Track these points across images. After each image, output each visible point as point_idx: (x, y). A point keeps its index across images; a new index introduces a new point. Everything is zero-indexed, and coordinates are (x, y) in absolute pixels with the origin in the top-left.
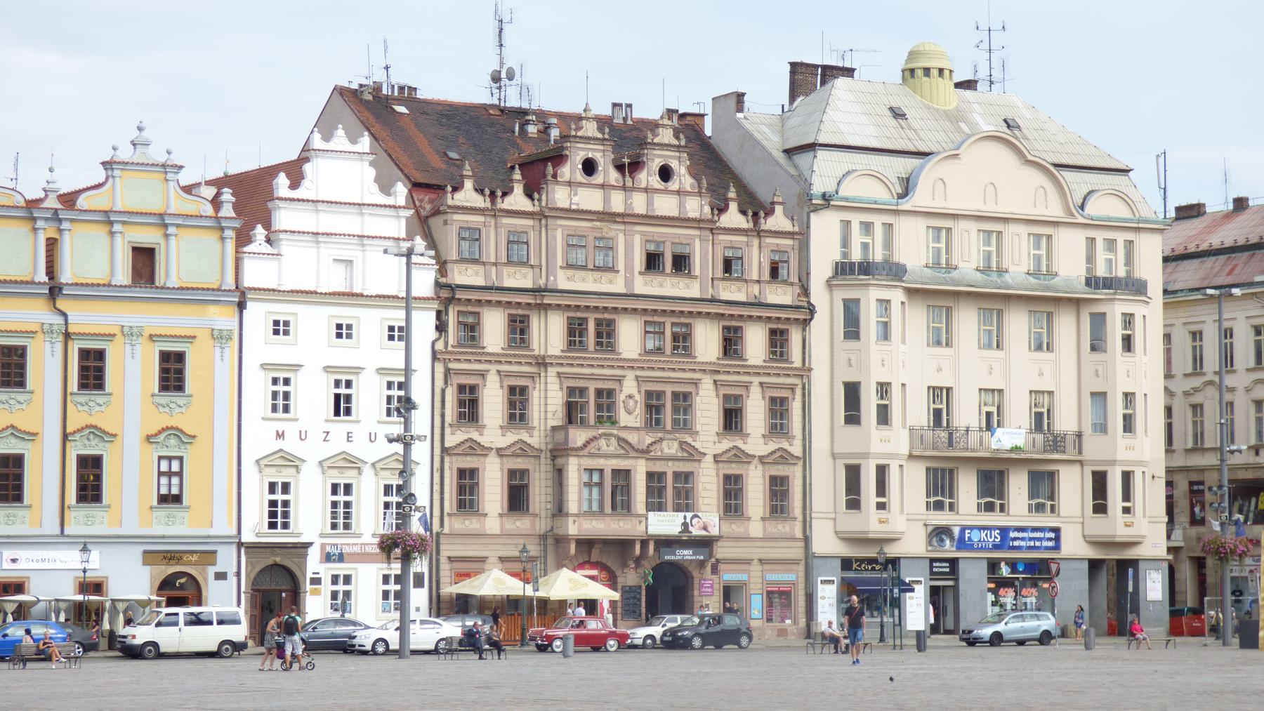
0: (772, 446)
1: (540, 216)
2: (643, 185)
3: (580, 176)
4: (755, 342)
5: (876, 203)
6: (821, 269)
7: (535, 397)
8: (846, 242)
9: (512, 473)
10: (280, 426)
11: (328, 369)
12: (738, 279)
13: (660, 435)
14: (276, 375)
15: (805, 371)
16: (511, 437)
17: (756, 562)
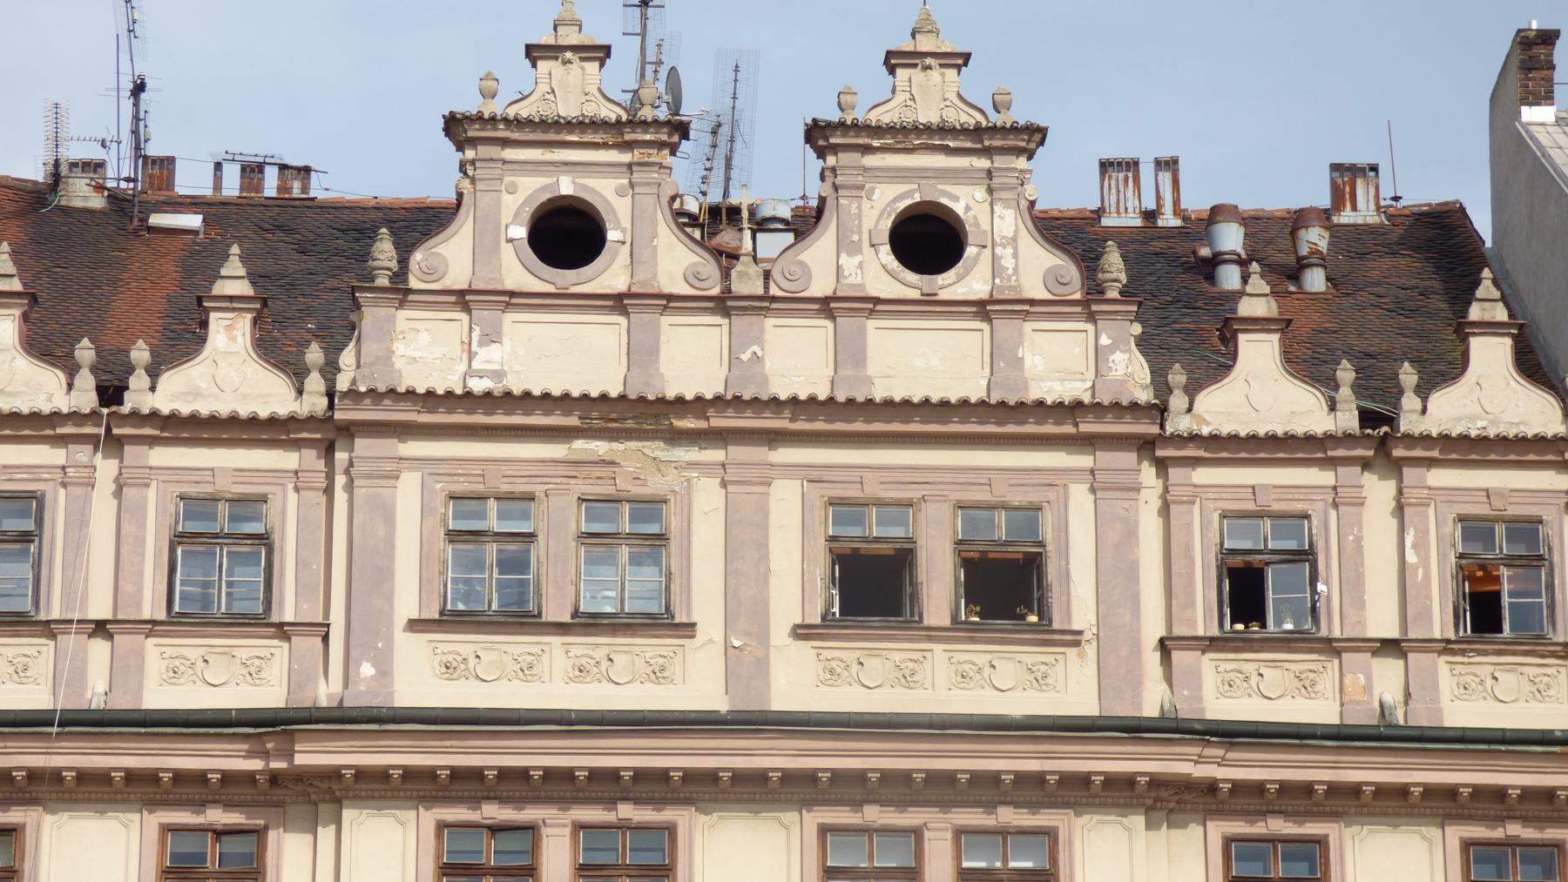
1: (328, 434)
2: (821, 286)
3: (518, 270)
12: (1288, 642)
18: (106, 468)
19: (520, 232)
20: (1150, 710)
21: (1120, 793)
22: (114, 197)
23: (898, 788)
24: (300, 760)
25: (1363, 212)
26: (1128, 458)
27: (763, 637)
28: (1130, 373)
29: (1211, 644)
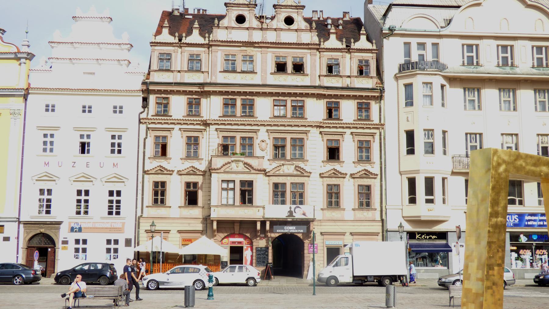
0: (360, 167)
1: (209, 46)
3: (234, 24)
4: (348, 110)
5: (425, 31)
6: (390, 67)
7: (203, 143)
8: (408, 53)
9: (188, 185)
10: (47, 160)
11: (76, 129)
12: (335, 76)
13: (282, 162)
14: (46, 132)
15: (381, 126)
16: (188, 164)
17: (348, 234)
18: (180, 50)
19: (235, 19)
20: (317, 85)
21: (313, 95)
22: (181, 14)
23: (284, 94)
24: (205, 89)
25: (347, 18)
26: (315, 51)
27: (266, 74)
28: (316, 40)
29: (326, 76)
